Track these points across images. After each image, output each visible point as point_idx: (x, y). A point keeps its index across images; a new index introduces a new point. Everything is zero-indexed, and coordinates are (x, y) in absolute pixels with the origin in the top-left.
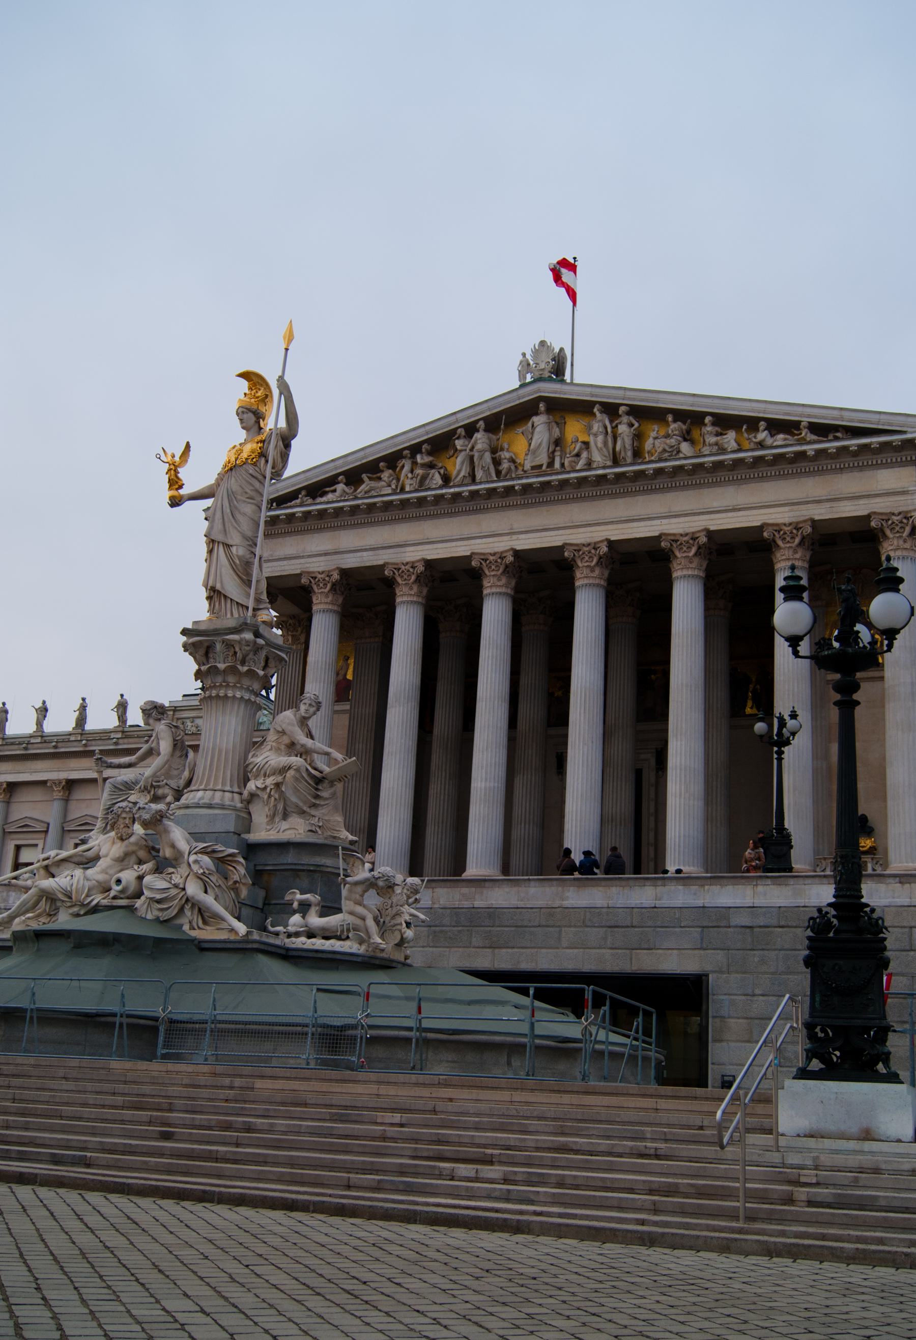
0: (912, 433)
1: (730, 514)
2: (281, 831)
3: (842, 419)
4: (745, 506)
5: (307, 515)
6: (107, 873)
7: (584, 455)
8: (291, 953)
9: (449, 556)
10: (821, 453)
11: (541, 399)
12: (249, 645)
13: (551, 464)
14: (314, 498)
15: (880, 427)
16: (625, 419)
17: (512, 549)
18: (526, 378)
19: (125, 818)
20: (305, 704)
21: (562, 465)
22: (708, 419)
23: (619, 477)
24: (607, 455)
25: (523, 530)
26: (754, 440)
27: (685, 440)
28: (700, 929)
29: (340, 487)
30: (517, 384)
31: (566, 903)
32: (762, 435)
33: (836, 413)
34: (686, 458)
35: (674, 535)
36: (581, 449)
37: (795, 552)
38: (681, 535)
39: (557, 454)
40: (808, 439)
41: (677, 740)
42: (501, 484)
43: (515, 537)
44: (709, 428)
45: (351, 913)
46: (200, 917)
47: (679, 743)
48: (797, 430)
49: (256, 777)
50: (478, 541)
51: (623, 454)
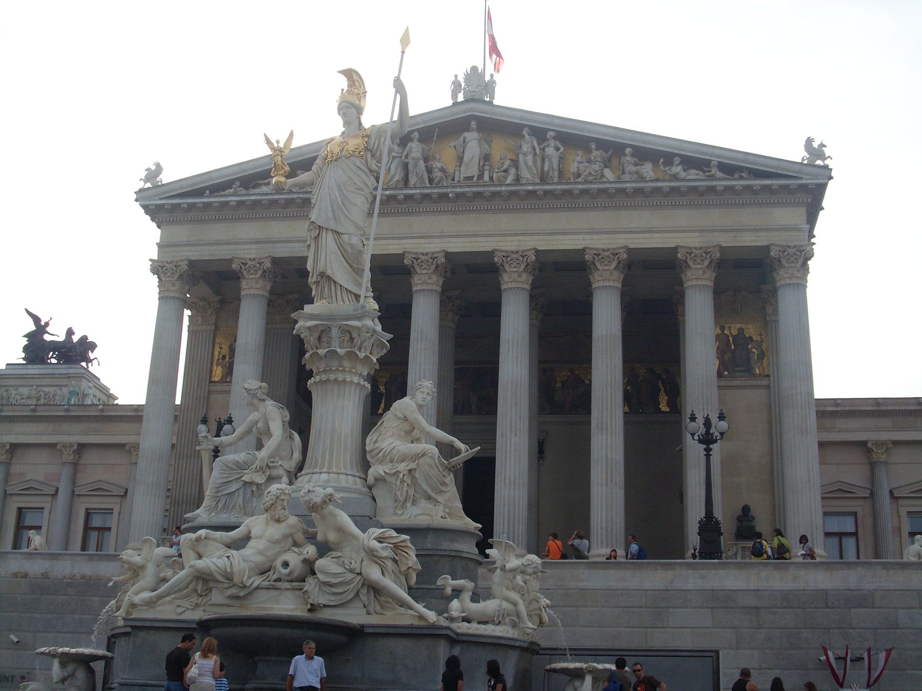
0: (806, 179)
1: (646, 235)
2: (413, 516)
3: (746, 161)
5: (241, 204)
6: (264, 555)
7: (513, 171)
8: (460, 638)
10: (730, 189)
12: (368, 332)
13: (481, 176)
14: (247, 188)
15: (779, 172)
16: (552, 143)
17: (444, 251)
18: (457, 97)
19: (283, 500)
20: (423, 392)
21: (491, 178)
22: (628, 150)
23: (546, 193)
24: (535, 172)
25: (454, 234)
26: (669, 172)
27: (606, 166)
28: (710, 610)
30: (450, 103)
31: (582, 585)
33: (741, 156)
34: (610, 182)
35: (597, 249)
36: (509, 166)
37: (704, 273)
38: (603, 250)
39: (487, 168)
40: (718, 176)
41: (602, 435)
42: (435, 191)
43: (445, 240)
44: (629, 158)
45: (506, 599)
46: (376, 601)
47: (604, 437)
49: (381, 462)
50: (410, 241)
51: (551, 173)
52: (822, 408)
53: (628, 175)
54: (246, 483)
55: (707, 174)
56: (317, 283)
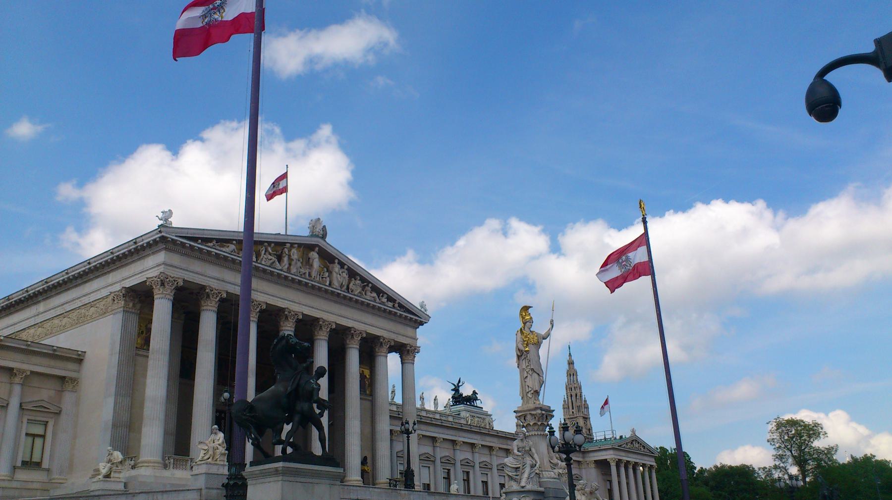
3: (407, 305)
9: (274, 304)
11: (317, 245)
15: (416, 313)
16: (346, 271)
22: (370, 285)
29: (232, 247)
43: (301, 306)
44: (369, 289)
52: (391, 415)
54: (536, 473)
56: (532, 393)
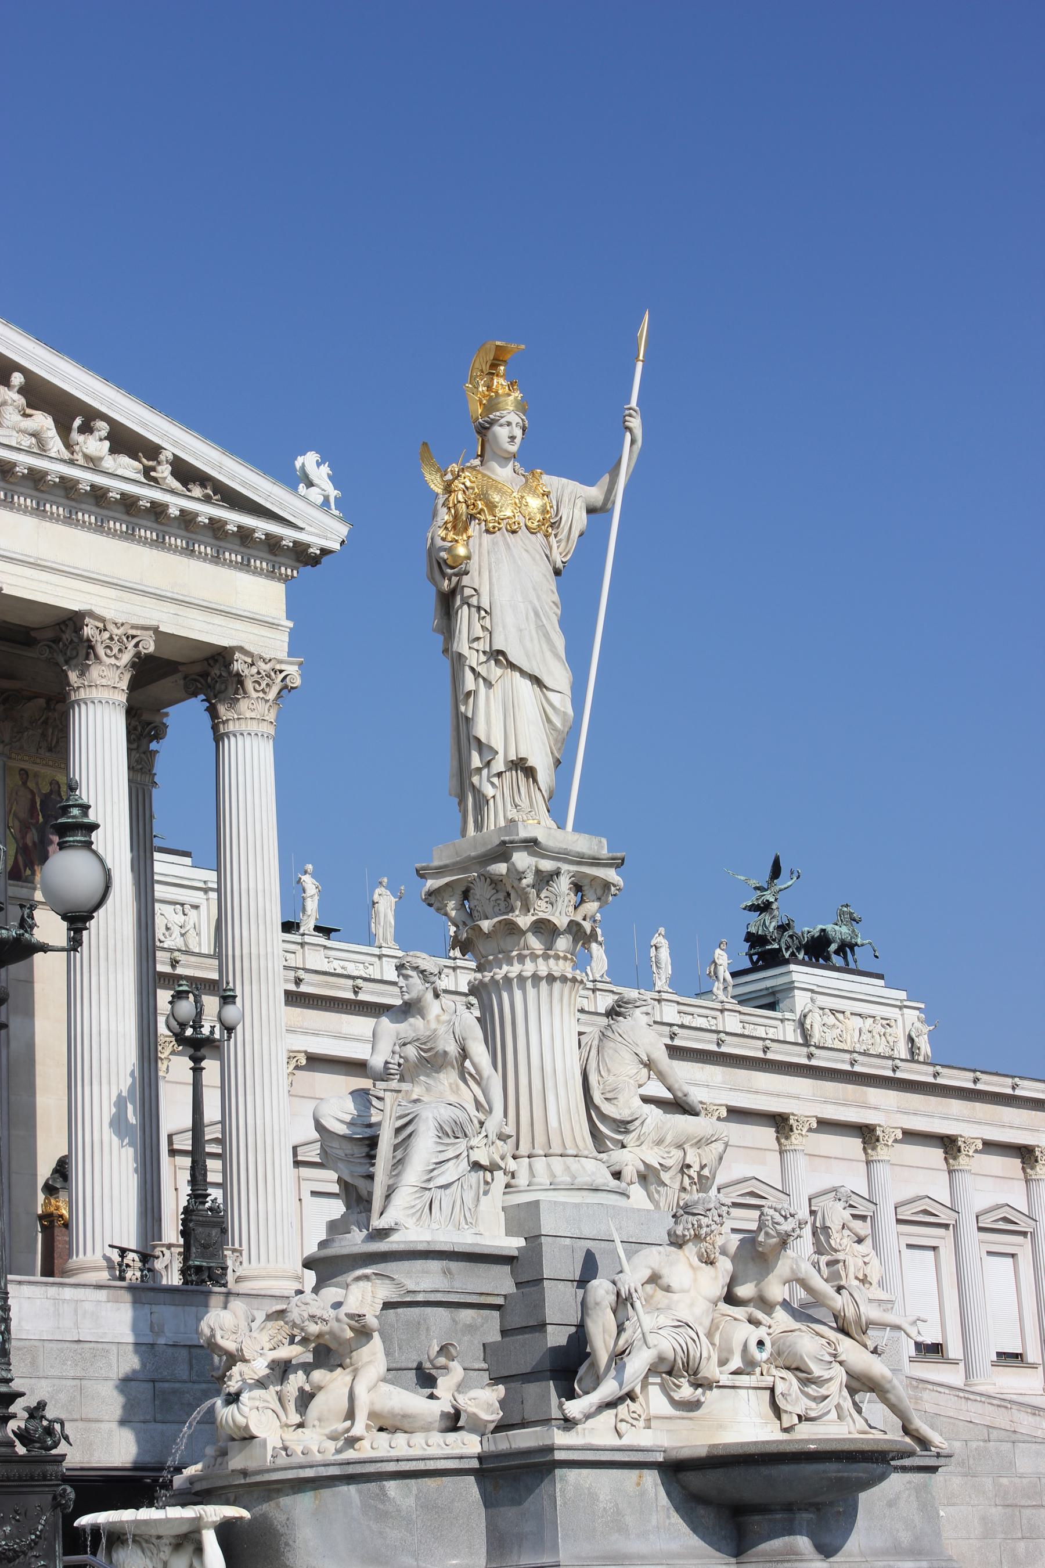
0: (310, 534)
4: (54, 566)
10: (187, 519)
22: (17, 379)
32: (95, 445)
48: (148, 460)
53: (15, 433)
55: (153, 474)
